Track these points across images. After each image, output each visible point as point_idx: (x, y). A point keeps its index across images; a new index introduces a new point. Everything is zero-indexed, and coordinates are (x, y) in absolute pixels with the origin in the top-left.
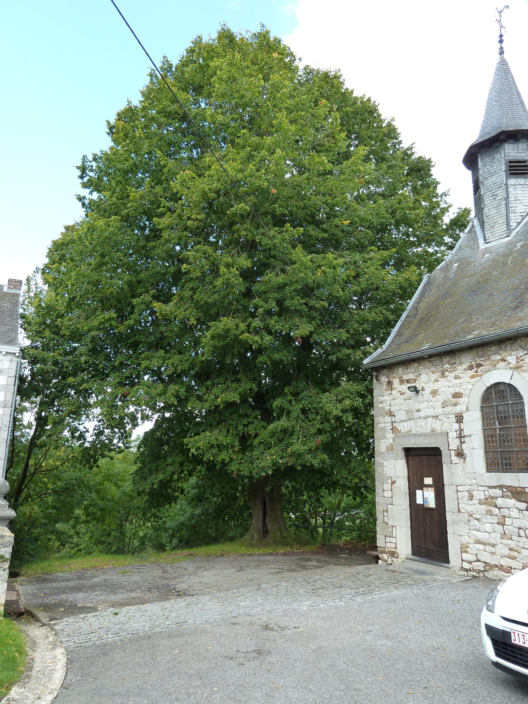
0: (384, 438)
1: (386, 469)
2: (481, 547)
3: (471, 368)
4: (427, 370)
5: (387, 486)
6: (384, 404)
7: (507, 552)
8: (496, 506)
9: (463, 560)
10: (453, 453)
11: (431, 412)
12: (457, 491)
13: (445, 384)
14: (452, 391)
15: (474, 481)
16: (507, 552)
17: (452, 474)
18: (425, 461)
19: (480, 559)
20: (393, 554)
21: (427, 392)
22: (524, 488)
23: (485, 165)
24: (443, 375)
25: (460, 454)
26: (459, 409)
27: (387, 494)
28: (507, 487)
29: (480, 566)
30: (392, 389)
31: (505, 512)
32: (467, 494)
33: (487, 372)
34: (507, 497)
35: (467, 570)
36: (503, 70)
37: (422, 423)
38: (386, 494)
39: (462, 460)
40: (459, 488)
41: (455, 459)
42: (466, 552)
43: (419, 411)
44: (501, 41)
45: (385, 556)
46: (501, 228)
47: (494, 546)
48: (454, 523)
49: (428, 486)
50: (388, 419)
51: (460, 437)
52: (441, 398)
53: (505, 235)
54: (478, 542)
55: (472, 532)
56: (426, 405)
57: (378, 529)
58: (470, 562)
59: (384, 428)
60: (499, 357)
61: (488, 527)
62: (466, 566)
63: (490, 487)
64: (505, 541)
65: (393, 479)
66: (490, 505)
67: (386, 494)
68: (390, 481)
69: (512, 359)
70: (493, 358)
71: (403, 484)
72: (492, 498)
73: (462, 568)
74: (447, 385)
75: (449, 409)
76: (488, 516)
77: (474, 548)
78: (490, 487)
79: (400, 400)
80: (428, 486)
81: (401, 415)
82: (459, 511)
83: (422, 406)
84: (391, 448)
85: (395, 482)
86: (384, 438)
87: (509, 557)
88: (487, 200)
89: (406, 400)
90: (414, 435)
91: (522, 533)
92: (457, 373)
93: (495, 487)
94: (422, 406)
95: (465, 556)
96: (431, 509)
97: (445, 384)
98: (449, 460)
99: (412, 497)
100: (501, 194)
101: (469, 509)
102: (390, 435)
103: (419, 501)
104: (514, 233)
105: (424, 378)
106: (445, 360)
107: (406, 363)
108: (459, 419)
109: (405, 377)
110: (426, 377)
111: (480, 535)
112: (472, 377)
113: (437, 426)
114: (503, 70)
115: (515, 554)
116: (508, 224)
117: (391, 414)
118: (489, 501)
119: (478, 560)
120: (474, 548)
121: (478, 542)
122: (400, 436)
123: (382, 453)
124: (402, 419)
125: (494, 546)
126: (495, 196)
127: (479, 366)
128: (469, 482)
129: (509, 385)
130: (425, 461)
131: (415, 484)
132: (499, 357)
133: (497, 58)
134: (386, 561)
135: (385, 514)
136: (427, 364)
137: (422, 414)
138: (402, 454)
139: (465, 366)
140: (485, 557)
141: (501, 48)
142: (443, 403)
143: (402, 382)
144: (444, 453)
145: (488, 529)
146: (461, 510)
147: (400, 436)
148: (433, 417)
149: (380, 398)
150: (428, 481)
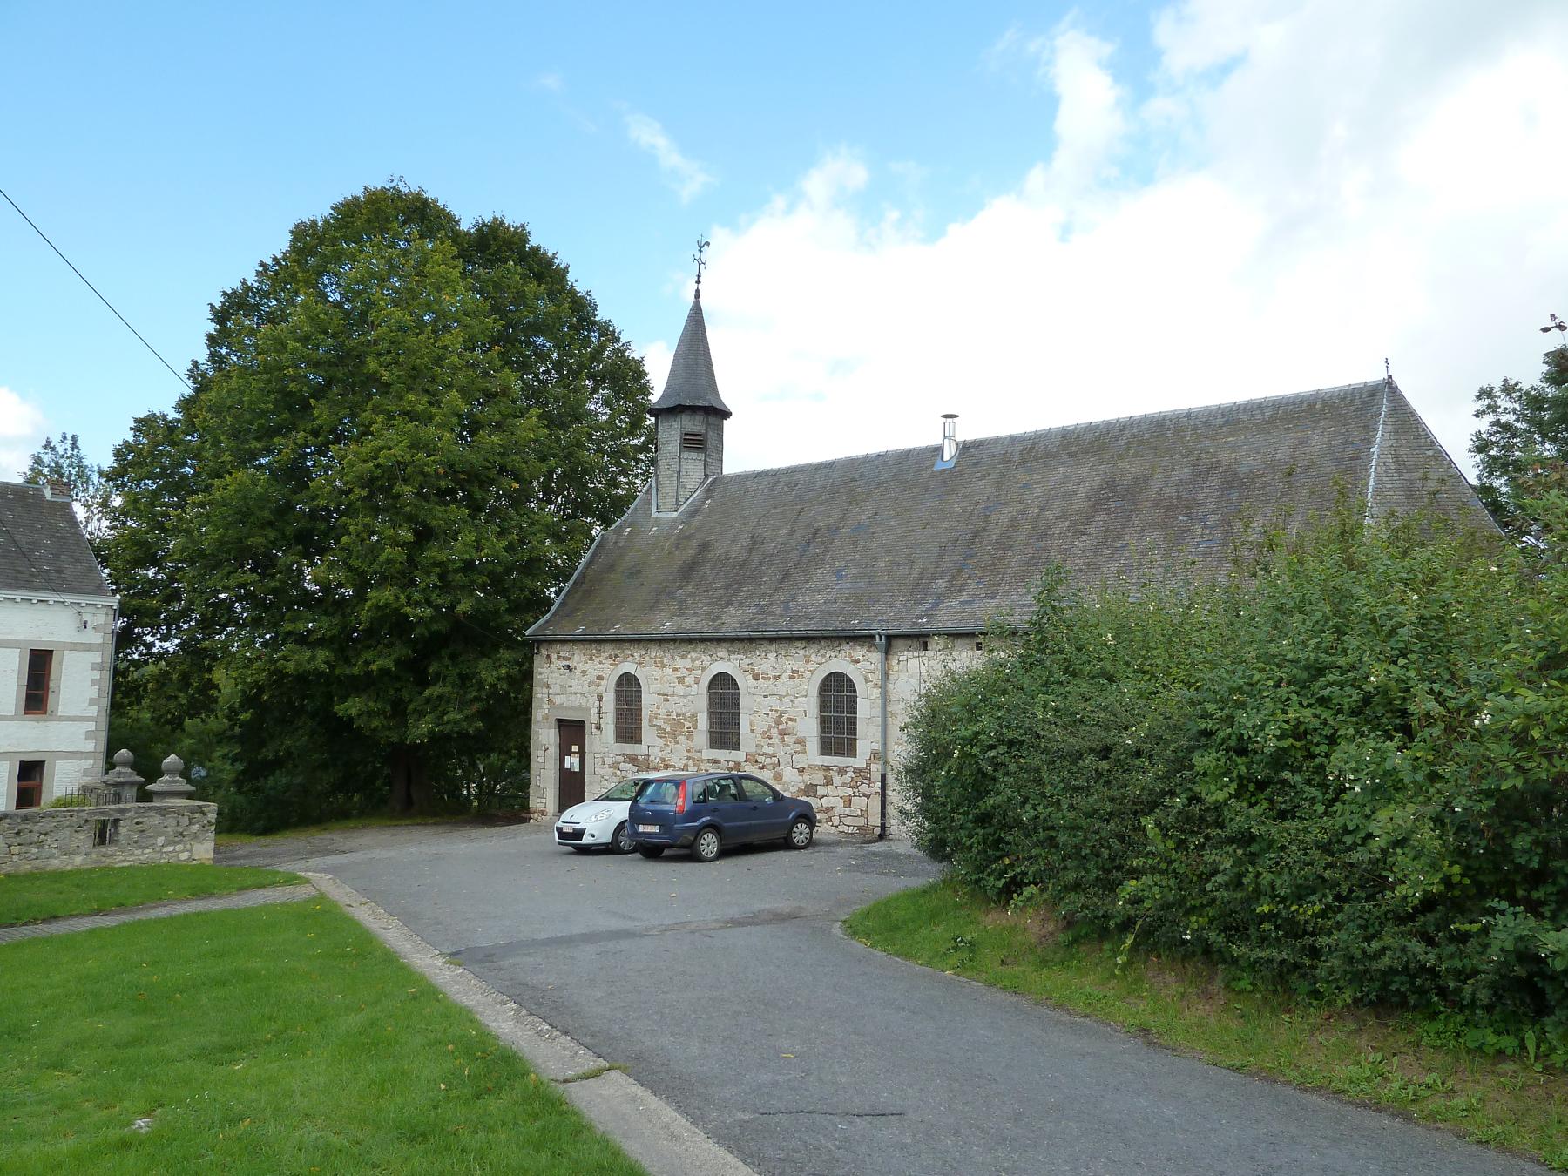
5: (541, 753)
14: (596, 673)
18: (572, 731)
20: (543, 813)
21: (578, 671)
25: (599, 727)
26: (601, 689)
27: (541, 760)
36: (696, 320)
37: (572, 698)
46: (671, 501)
50: (545, 690)
52: (588, 678)
56: (577, 683)
69: (637, 656)
71: (554, 750)
81: (556, 689)
83: (574, 683)
84: (546, 718)
94: (574, 683)
98: (590, 729)
100: (675, 467)
102: (546, 706)
103: (567, 766)
105: (576, 657)
108: (600, 700)
110: (579, 658)
117: (548, 687)
118: (615, 766)
130: (572, 731)
131: (564, 751)
136: (580, 646)
138: (554, 723)
150: (575, 748)
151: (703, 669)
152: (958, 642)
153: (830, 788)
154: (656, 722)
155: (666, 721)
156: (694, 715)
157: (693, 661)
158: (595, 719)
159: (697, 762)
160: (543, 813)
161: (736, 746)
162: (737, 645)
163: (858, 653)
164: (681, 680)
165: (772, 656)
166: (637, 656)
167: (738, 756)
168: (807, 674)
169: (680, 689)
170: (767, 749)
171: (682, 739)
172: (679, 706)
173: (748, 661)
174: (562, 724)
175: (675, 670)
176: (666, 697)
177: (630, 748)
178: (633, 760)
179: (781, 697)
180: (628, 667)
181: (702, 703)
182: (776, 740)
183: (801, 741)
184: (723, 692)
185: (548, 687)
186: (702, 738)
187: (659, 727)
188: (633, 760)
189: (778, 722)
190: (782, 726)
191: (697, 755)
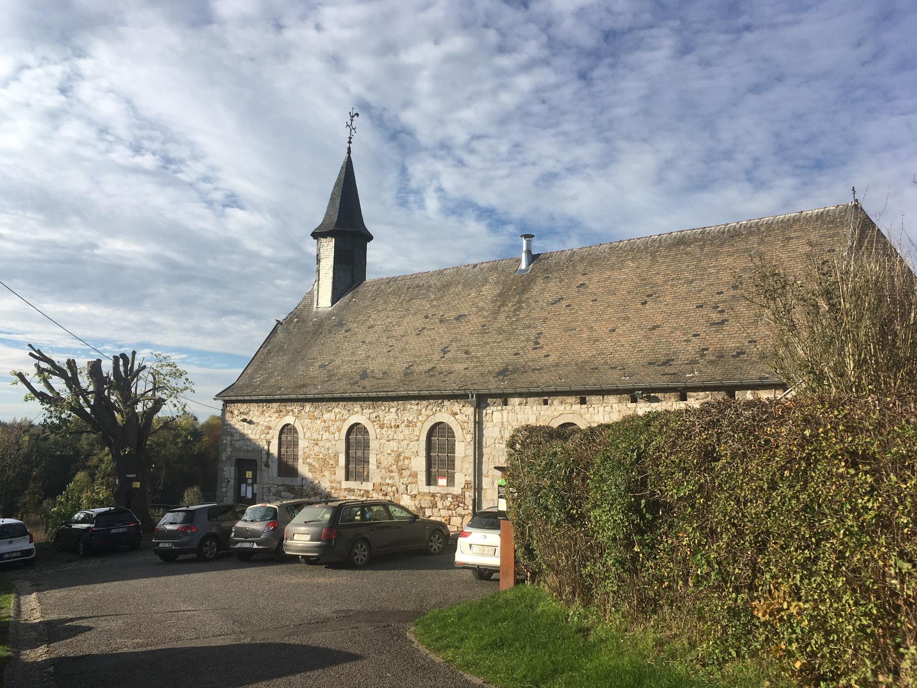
3: (277, 412)
5: (224, 485)
25: (267, 465)
26: (269, 437)
27: (224, 490)
44: (350, 142)
50: (229, 438)
84: (229, 458)
127: (281, 411)
133: (346, 155)
141: (349, 148)
152: (530, 400)
153: (435, 510)
154: (310, 461)
156: (336, 455)
161: (367, 479)
163: (456, 407)
165: (393, 410)
166: (296, 411)
167: (368, 486)
168: (419, 424)
169: (326, 435)
170: (388, 481)
171: (327, 473)
173: (374, 415)
177: (288, 481)
179: (399, 441)
180: (289, 419)
181: (342, 446)
182: (395, 474)
183: (415, 475)
184: (356, 439)
186: (341, 473)
187: (310, 465)
189: (397, 461)
190: (400, 462)
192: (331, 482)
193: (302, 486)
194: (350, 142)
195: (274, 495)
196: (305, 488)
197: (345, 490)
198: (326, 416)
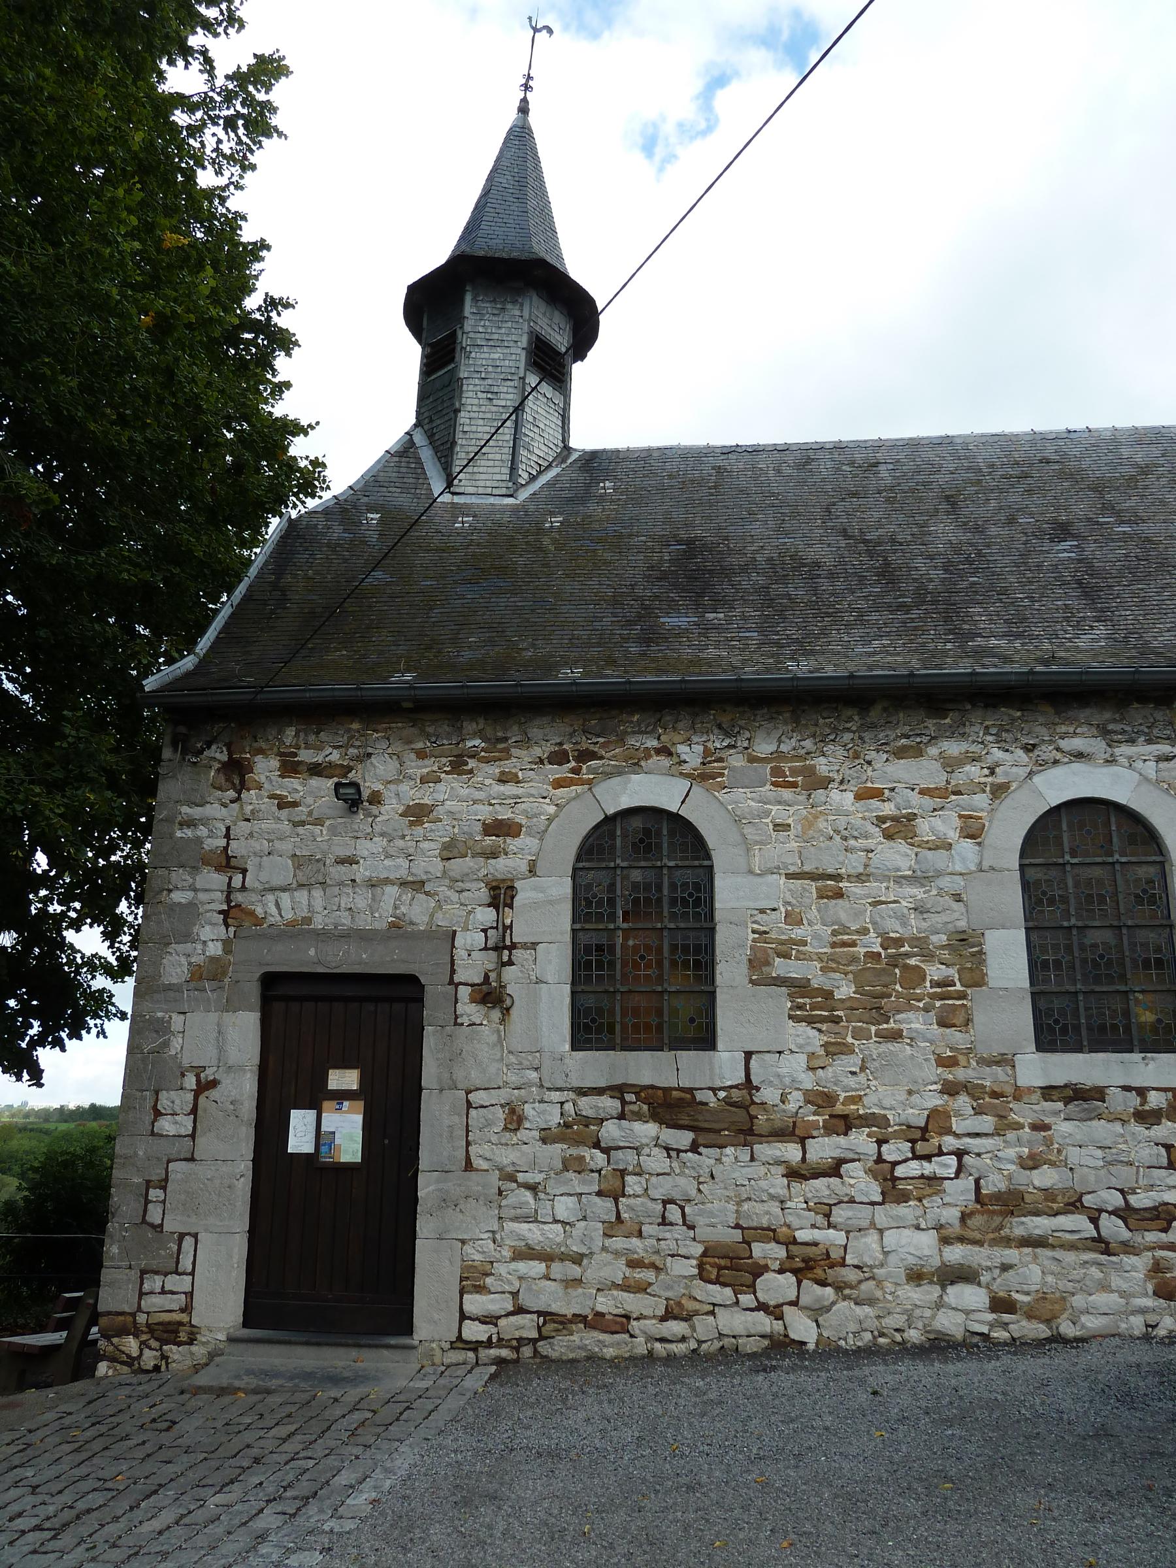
0: (187, 937)
1: (176, 1043)
2: (538, 1268)
3: (558, 758)
4: (397, 747)
6: (202, 831)
7: (619, 1271)
8: (597, 1145)
9: (463, 1317)
10: (464, 992)
11: (398, 868)
12: (469, 1105)
13: (464, 792)
14: (484, 813)
15: (534, 1075)
16: (619, 1271)
17: (455, 1057)
18: (349, 1019)
19: (526, 1300)
21: (390, 809)
22: (690, 1090)
23: (479, 314)
24: (458, 766)
25: (491, 996)
26: (500, 867)
28: (638, 1090)
29: (526, 1326)
30: (242, 787)
31: (626, 1159)
32: (500, 1114)
33: (608, 775)
34: (638, 1117)
35: (475, 1346)
36: (519, 146)
38: (166, 1125)
39: (496, 1014)
40: (477, 1098)
41: (469, 1010)
42: (480, 1289)
43: (351, 861)
44: (527, 87)
45: (131, 1345)
47: (578, 1259)
48: (446, 1202)
49: (341, 1096)
50: (214, 879)
51: (503, 946)
52: (439, 832)
53: (504, 491)
54: (526, 1253)
55: (510, 1226)
57: (112, 1249)
58: (489, 1320)
59: (192, 905)
60: (652, 743)
61: (565, 1207)
62: (474, 1331)
63: (582, 1092)
64: (618, 1243)
65: (209, 1074)
66: (578, 1142)
67: (166, 1125)
68: (190, 1081)
69: (691, 754)
70: (632, 741)
71: (241, 1089)
72: (586, 1121)
73: (460, 1343)
74: (462, 800)
75: (458, 866)
76: (571, 1175)
77: (508, 1272)
78: (582, 1092)
79: (276, 823)
80: (341, 1096)
82: (469, 1166)
83: (364, 848)
84: (209, 974)
85: (214, 1084)
86: (187, 937)
87: (626, 1287)
88: (472, 397)
89: (296, 824)
90: (322, 936)
91: (674, 1213)
92: (508, 765)
93: (599, 1091)
94: (364, 848)
95: (475, 1303)
96: (349, 1168)
97: (464, 792)
99: (269, 1129)
100: (509, 398)
101: (507, 1157)
103: (300, 1140)
104: (523, 495)
106: (470, 727)
107: (320, 713)
108: (501, 895)
109: (306, 756)
111: (532, 1233)
112: (558, 784)
113: (418, 911)
114: (519, 146)
115: (649, 1275)
116: (513, 469)
117: (226, 863)
118: (577, 1131)
119: (520, 1310)
120: (508, 1272)
121: (526, 1253)
122: (262, 936)
123: (170, 988)
124: (277, 881)
125: (578, 1259)
126: (491, 395)
127: (585, 756)
128: (513, 1078)
129: (675, 819)
132: (652, 743)
133: (510, 116)
134: (130, 1361)
135: (154, 1194)
137: (362, 872)
138: (253, 991)
139: (549, 748)
140: (551, 1297)
141: (524, 101)
142: (446, 847)
143: (290, 768)
144: (434, 990)
145: (567, 1211)
146: (477, 1162)
147: (262, 936)
148: (404, 884)
149: (185, 809)
150: (344, 1079)
151: (999, 791)
154: (780, 967)
155: (829, 965)
156: (967, 947)
157: (950, 765)
158: (472, 966)
159: (995, 1102)
160: (169, 1333)
162: (1138, 714)
164: (899, 827)
169: (897, 856)
171: (914, 1022)
172: (886, 908)
174: (281, 994)
175: (864, 795)
176: (830, 884)
177: (650, 1068)
178: (669, 1106)
180: (651, 788)
181: (1012, 899)
185: (226, 863)
187: (799, 987)
188: (669, 1106)
191: (990, 1077)
192: (942, 1062)
193: (748, 1084)
194: (527, 87)
195: (547, 1137)
196: (768, 1095)
197: (1048, 1092)
198: (887, 770)
